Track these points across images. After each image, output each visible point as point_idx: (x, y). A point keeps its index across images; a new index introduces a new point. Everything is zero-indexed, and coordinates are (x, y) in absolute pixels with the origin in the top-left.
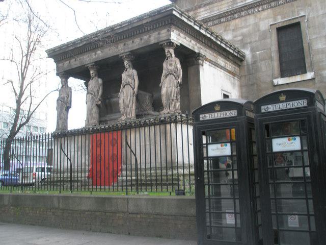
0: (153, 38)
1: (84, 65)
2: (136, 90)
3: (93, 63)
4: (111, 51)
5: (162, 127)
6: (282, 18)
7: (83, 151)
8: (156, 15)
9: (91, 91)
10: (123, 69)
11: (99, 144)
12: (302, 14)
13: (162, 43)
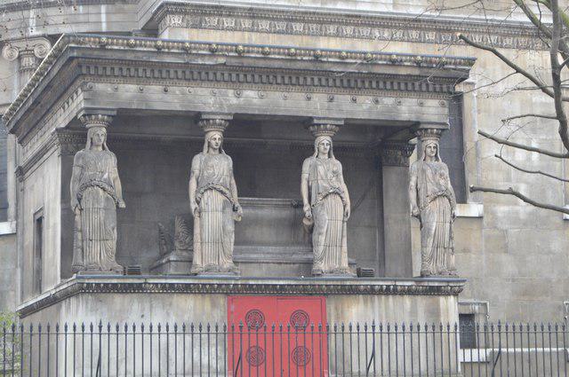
2: (348, 208)
3: (230, 114)
11: (255, 321)
13: (426, 126)
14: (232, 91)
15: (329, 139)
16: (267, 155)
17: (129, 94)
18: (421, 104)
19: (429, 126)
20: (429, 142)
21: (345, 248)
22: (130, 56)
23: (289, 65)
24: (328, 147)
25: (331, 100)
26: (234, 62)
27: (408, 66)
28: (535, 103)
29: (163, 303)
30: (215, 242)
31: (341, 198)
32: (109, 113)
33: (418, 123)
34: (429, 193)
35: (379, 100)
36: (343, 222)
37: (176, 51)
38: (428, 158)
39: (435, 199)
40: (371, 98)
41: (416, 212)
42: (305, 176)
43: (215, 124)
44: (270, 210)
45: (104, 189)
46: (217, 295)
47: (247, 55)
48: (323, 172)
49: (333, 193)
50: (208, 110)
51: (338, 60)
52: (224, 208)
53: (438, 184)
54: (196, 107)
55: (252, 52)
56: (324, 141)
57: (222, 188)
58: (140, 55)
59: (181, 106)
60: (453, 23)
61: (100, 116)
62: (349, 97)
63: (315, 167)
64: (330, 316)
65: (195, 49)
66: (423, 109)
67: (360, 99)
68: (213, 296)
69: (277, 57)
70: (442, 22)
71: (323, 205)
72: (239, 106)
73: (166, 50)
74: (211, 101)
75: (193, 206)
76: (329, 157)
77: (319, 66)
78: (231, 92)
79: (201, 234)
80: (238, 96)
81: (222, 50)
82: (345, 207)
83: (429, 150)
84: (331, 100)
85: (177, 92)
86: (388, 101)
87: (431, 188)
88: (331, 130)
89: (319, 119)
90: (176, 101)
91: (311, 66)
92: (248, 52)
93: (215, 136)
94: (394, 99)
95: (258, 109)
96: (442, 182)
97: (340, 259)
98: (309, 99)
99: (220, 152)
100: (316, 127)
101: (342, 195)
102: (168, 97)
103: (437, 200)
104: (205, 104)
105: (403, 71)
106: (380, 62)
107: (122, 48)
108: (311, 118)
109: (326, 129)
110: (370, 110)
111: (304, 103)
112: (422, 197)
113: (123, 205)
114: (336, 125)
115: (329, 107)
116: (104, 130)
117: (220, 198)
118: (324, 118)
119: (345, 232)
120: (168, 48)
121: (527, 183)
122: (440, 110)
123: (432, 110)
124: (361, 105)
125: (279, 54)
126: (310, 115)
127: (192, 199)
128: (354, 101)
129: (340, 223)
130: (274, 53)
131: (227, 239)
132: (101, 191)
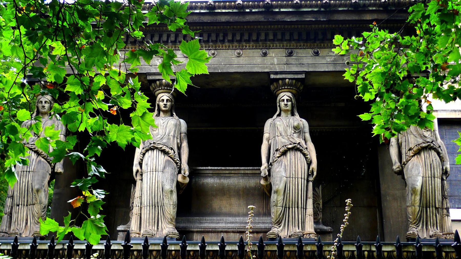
2: (314, 165)
4: (242, 60)
15: (289, 94)
21: (310, 209)
23: (236, 18)
24: (289, 103)
27: (373, 11)
31: (304, 155)
36: (308, 181)
42: (266, 136)
43: (161, 85)
44: (235, 179)
48: (283, 129)
50: (153, 71)
52: (164, 168)
56: (285, 96)
57: (164, 148)
62: (310, 51)
63: (274, 126)
69: (224, 11)
75: (136, 168)
89: (276, 73)
91: (261, 18)
97: (303, 223)
98: (265, 55)
100: (275, 84)
101: (306, 152)
106: (340, 9)
108: (268, 73)
109: (285, 84)
112: (403, 151)
115: (287, 61)
117: (162, 158)
118: (281, 73)
124: (324, 57)
126: (266, 70)
127: (136, 162)
128: (317, 54)
129: (301, 183)
131: (166, 201)
132: (34, 156)
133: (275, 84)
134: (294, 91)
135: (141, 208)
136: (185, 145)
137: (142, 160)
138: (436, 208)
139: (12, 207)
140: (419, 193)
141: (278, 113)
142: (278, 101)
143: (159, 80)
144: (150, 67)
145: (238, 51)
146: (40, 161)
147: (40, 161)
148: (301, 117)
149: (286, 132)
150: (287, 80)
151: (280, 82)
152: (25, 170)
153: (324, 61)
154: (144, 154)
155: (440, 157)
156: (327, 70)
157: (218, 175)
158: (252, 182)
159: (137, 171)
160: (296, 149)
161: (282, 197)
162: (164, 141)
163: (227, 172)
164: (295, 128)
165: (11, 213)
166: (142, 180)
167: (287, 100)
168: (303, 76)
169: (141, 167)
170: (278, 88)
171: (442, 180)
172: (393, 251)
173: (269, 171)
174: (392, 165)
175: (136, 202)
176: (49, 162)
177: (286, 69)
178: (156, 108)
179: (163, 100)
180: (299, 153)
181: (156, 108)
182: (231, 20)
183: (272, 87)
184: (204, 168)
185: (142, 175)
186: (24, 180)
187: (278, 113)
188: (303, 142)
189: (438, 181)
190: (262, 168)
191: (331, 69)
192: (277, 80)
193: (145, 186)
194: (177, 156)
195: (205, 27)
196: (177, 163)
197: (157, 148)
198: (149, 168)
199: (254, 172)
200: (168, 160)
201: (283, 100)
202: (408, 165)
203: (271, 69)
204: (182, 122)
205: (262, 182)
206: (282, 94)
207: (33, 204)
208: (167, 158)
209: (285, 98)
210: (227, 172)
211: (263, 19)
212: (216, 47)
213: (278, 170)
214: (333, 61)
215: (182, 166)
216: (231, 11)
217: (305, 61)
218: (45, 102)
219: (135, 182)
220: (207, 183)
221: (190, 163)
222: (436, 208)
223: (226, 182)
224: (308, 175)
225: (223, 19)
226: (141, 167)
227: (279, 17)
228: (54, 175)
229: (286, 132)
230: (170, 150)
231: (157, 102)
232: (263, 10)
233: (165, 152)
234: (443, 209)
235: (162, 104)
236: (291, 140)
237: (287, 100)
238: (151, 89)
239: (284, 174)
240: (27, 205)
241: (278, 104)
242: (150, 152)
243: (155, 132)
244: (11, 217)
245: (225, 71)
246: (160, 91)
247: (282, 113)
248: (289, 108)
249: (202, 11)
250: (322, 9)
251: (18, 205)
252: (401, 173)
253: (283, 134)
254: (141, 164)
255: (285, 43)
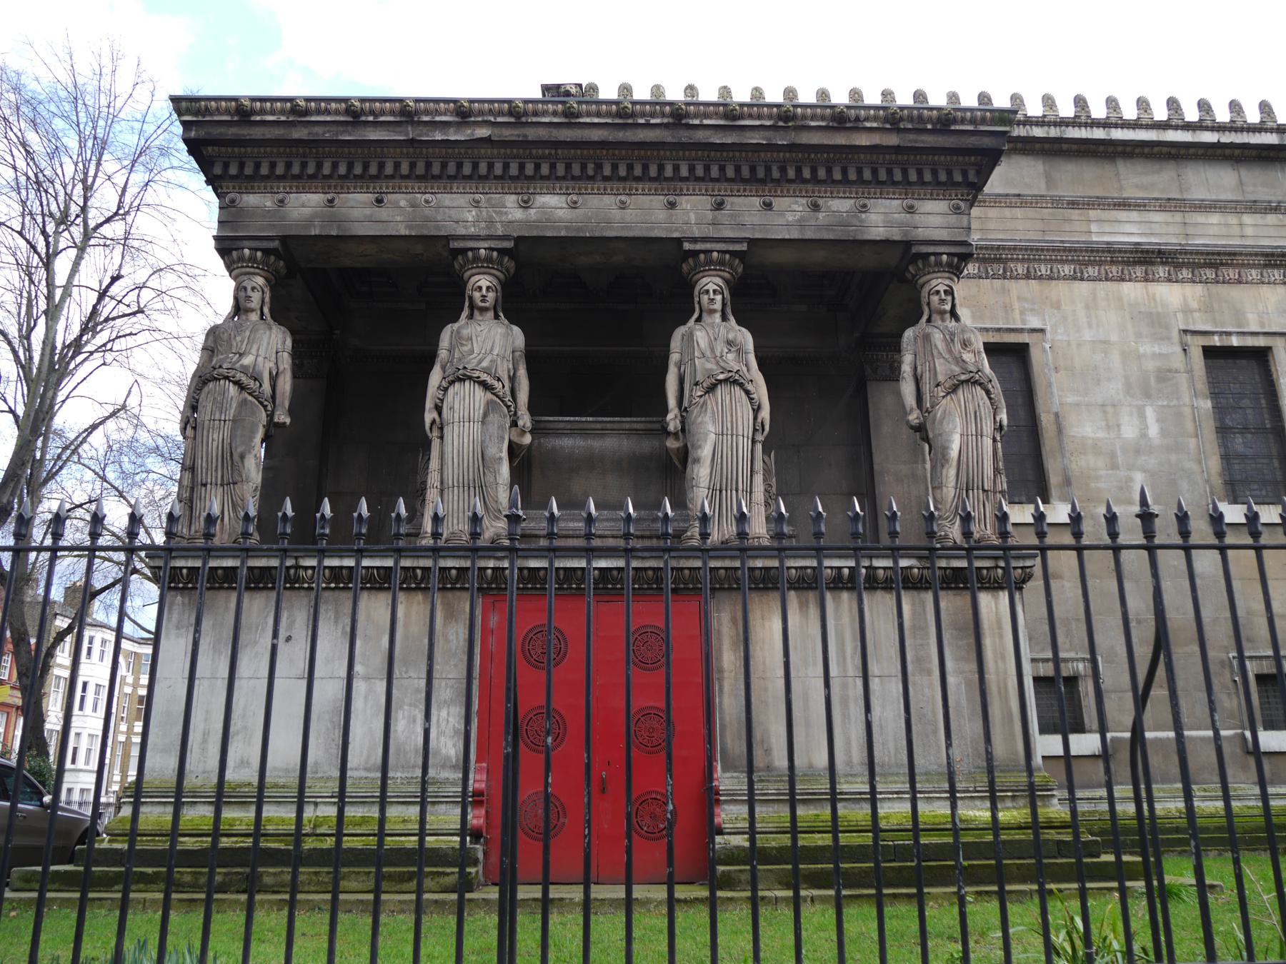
0: (882, 217)
1: (447, 238)
2: (765, 413)
5: (952, 603)
6: (974, 317)
7: (411, 681)
8: (926, 131)
9: (486, 371)
10: (682, 306)
12: (1035, 323)
13: (925, 249)
14: (513, 197)
15: (719, 281)
16: (599, 332)
17: (307, 211)
18: (910, 210)
19: (931, 249)
20: (934, 282)
22: (299, 133)
24: (719, 298)
25: (719, 206)
26: (508, 134)
27: (871, 129)
28: (1144, 355)
29: (337, 612)
30: (466, 486)
31: (748, 393)
32: (265, 244)
33: (907, 244)
34: (941, 378)
35: (821, 201)
36: (754, 442)
37: (391, 119)
38: (935, 317)
39: (954, 389)
40: (804, 201)
41: (914, 417)
42: (674, 357)
43: (477, 259)
45: (238, 383)
46: (458, 593)
47: (535, 119)
49: (726, 380)
51: (722, 122)
52: (485, 415)
53: (960, 361)
54: (438, 228)
55: (545, 113)
56: (711, 286)
57: (484, 377)
58: (318, 130)
59: (406, 227)
60: (1004, 248)
61: (247, 251)
64: (720, 639)
65: (427, 112)
66: (916, 217)
67: (778, 203)
68: (449, 595)
69: (596, 120)
70: (987, 248)
71: (705, 403)
72: (526, 223)
73: (371, 118)
74: (470, 216)
75: (429, 416)
76: (724, 318)
77: (684, 136)
78: (511, 200)
79: (441, 470)
80: (525, 205)
81: (481, 113)
82: (756, 411)
83: (935, 299)
84: (719, 206)
85: (403, 203)
86: (840, 205)
87: (943, 369)
88: (721, 263)
89: (694, 240)
90: (398, 218)
92: (536, 114)
93: (483, 284)
94: (852, 201)
95: (567, 228)
96: (968, 357)
98: (672, 205)
99: (497, 317)
100: (691, 261)
101: (750, 387)
102: (383, 213)
103: (960, 392)
104: (457, 222)
105: (863, 140)
106: (813, 124)
107: (283, 118)
108: (679, 241)
109: (710, 262)
110: (801, 224)
111: (661, 215)
112: (926, 388)
113: (283, 417)
114: (732, 253)
116: (260, 281)
117: (480, 396)
118: (704, 240)
119: (759, 465)
120: (372, 112)
121: (1145, 471)
122: (953, 219)
123: (937, 220)
124: (782, 213)
125: (598, 114)
126: (676, 235)
127: (429, 404)
128: (768, 206)
129: (744, 444)
130: (589, 114)
132: (233, 390)
133: (691, 261)
134: (727, 275)
135: (442, 490)
136: (522, 372)
137: (442, 401)
138: (984, 490)
139: (192, 489)
140: (955, 463)
141: (696, 315)
142: (696, 293)
143: (471, 249)
144: (455, 225)
145: (623, 198)
146: (245, 401)
147: (245, 401)
148: (739, 323)
149: (712, 350)
150: (715, 254)
151: (702, 256)
152: (217, 417)
153: (781, 221)
154: (446, 390)
155: (990, 399)
156: (787, 237)
157: (583, 432)
158: (646, 445)
159: (433, 422)
160: (734, 381)
161: (708, 470)
162: (484, 364)
163: (599, 426)
164: (730, 343)
165: (191, 500)
166: (442, 438)
167: (715, 291)
168: (744, 247)
169: (440, 414)
170: (698, 270)
171: (994, 440)
172: (911, 568)
173: (683, 423)
174: (906, 414)
175: (433, 478)
176: (261, 403)
177: (712, 233)
178: (467, 304)
179: (480, 288)
180: (737, 388)
181: (467, 304)
182: (611, 139)
183: (685, 267)
184: (556, 418)
185: (441, 429)
186: (215, 436)
187: (696, 315)
188: (745, 369)
189: (988, 442)
190: (670, 416)
191: (795, 235)
192: (695, 254)
193: (448, 449)
194: (508, 393)
195: (560, 152)
196: (508, 407)
197: (470, 378)
198: (456, 416)
199: (649, 426)
200: (492, 401)
201: (707, 292)
202: (935, 415)
203: (684, 231)
204: (516, 329)
205: (672, 444)
206: (705, 280)
207: (235, 483)
208: (489, 396)
209: (711, 287)
210: (599, 426)
211: (669, 139)
212: (580, 189)
213: (700, 419)
214: (799, 220)
215: (519, 413)
216: (609, 121)
217: (747, 220)
218: (253, 289)
219: (427, 445)
220: (562, 447)
221: (532, 408)
222: (984, 490)
223: (596, 444)
224: (755, 430)
225: (596, 135)
226: (440, 414)
227: (701, 136)
228: (272, 425)
229: (712, 350)
230: (496, 384)
231: (468, 292)
232: (671, 120)
233: (486, 386)
234: (995, 492)
235: (477, 295)
236: (722, 364)
237: (715, 291)
238: (456, 266)
239: (711, 428)
240: (222, 485)
241: (696, 299)
242: (457, 385)
243: (465, 349)
244: (191, 508)
245: (597, 234)
246: (474, 271)
247: (704, 315)
248: (718, 306)
249: (556, 120)
250: (781, 124)
251: (205, 485)
252: (920, 429)
253: (708, 354)
254: (439, 409)
255: (710, 185)
